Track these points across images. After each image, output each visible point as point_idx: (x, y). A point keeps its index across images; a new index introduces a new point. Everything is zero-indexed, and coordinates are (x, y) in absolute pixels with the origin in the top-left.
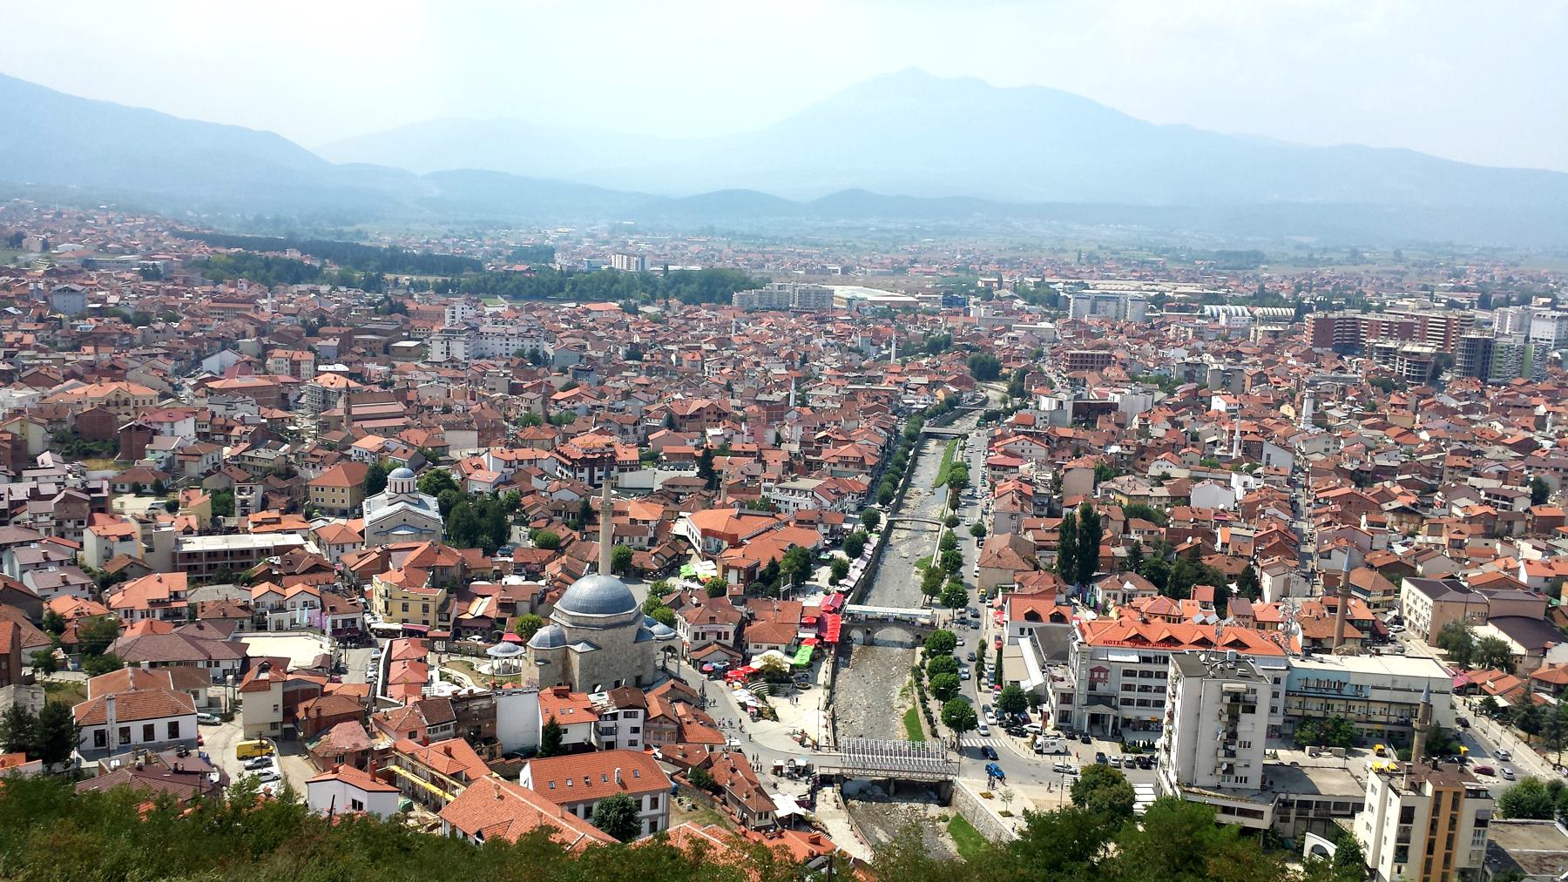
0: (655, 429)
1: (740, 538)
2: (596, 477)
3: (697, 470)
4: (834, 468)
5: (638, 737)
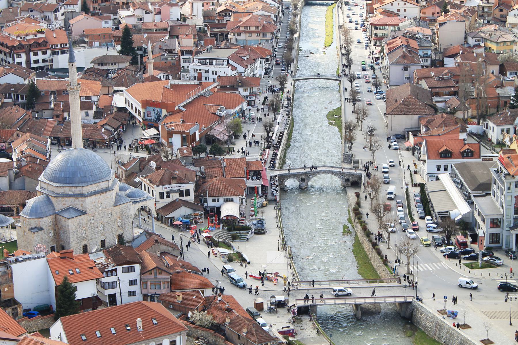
0: (73, 14)
2: (32, 62)
3: (119, 48)
4: (239, 38)
5: (136, 288)
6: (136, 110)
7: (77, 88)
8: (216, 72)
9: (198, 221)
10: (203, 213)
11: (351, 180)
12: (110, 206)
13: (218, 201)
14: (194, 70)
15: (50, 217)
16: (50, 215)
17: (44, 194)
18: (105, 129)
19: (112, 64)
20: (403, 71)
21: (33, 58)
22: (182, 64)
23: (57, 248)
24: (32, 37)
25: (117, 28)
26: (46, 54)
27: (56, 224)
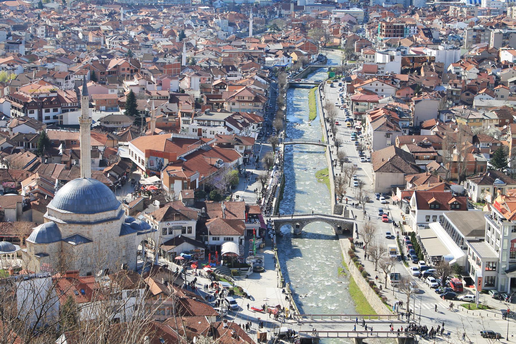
2: (44, 118)
4: (233, 107)
6: (139, 160)
7: (88, 121)
8: (214, 132)
9: (199, 258)
10: (204, 249)
11: (343, 228)
12: (116, 236)
13: (218, 239)
14: (193, 129)
15: (56, 243)
16: (56, 241)
17: (51, 221)
18: (110, 174)
19: (117, 123)
20: (385, 138)
21: (44, 114)
22: (182, 125)
24: (45, 95)
25: (122, 96)
26: (57, 111)
27: (62, 251)
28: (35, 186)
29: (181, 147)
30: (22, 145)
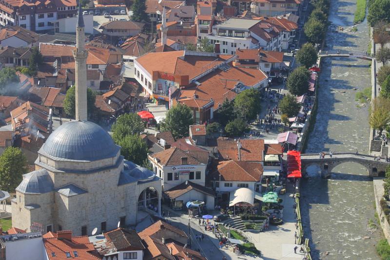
1: (190, 80)
2: (37, 25)
3: (131, 13)
4: (262, 8)
6: (146, 82)
8: (235, 44)
11: (379, 170)
13: (231, 186)
15: (49, 193)
21: (38, 21)
23: (54, 227)
27: (55, 202)
28: (26, 118)
29: (194, 65)
30: (12, 62)
